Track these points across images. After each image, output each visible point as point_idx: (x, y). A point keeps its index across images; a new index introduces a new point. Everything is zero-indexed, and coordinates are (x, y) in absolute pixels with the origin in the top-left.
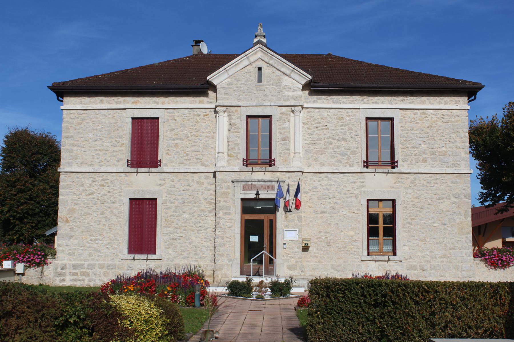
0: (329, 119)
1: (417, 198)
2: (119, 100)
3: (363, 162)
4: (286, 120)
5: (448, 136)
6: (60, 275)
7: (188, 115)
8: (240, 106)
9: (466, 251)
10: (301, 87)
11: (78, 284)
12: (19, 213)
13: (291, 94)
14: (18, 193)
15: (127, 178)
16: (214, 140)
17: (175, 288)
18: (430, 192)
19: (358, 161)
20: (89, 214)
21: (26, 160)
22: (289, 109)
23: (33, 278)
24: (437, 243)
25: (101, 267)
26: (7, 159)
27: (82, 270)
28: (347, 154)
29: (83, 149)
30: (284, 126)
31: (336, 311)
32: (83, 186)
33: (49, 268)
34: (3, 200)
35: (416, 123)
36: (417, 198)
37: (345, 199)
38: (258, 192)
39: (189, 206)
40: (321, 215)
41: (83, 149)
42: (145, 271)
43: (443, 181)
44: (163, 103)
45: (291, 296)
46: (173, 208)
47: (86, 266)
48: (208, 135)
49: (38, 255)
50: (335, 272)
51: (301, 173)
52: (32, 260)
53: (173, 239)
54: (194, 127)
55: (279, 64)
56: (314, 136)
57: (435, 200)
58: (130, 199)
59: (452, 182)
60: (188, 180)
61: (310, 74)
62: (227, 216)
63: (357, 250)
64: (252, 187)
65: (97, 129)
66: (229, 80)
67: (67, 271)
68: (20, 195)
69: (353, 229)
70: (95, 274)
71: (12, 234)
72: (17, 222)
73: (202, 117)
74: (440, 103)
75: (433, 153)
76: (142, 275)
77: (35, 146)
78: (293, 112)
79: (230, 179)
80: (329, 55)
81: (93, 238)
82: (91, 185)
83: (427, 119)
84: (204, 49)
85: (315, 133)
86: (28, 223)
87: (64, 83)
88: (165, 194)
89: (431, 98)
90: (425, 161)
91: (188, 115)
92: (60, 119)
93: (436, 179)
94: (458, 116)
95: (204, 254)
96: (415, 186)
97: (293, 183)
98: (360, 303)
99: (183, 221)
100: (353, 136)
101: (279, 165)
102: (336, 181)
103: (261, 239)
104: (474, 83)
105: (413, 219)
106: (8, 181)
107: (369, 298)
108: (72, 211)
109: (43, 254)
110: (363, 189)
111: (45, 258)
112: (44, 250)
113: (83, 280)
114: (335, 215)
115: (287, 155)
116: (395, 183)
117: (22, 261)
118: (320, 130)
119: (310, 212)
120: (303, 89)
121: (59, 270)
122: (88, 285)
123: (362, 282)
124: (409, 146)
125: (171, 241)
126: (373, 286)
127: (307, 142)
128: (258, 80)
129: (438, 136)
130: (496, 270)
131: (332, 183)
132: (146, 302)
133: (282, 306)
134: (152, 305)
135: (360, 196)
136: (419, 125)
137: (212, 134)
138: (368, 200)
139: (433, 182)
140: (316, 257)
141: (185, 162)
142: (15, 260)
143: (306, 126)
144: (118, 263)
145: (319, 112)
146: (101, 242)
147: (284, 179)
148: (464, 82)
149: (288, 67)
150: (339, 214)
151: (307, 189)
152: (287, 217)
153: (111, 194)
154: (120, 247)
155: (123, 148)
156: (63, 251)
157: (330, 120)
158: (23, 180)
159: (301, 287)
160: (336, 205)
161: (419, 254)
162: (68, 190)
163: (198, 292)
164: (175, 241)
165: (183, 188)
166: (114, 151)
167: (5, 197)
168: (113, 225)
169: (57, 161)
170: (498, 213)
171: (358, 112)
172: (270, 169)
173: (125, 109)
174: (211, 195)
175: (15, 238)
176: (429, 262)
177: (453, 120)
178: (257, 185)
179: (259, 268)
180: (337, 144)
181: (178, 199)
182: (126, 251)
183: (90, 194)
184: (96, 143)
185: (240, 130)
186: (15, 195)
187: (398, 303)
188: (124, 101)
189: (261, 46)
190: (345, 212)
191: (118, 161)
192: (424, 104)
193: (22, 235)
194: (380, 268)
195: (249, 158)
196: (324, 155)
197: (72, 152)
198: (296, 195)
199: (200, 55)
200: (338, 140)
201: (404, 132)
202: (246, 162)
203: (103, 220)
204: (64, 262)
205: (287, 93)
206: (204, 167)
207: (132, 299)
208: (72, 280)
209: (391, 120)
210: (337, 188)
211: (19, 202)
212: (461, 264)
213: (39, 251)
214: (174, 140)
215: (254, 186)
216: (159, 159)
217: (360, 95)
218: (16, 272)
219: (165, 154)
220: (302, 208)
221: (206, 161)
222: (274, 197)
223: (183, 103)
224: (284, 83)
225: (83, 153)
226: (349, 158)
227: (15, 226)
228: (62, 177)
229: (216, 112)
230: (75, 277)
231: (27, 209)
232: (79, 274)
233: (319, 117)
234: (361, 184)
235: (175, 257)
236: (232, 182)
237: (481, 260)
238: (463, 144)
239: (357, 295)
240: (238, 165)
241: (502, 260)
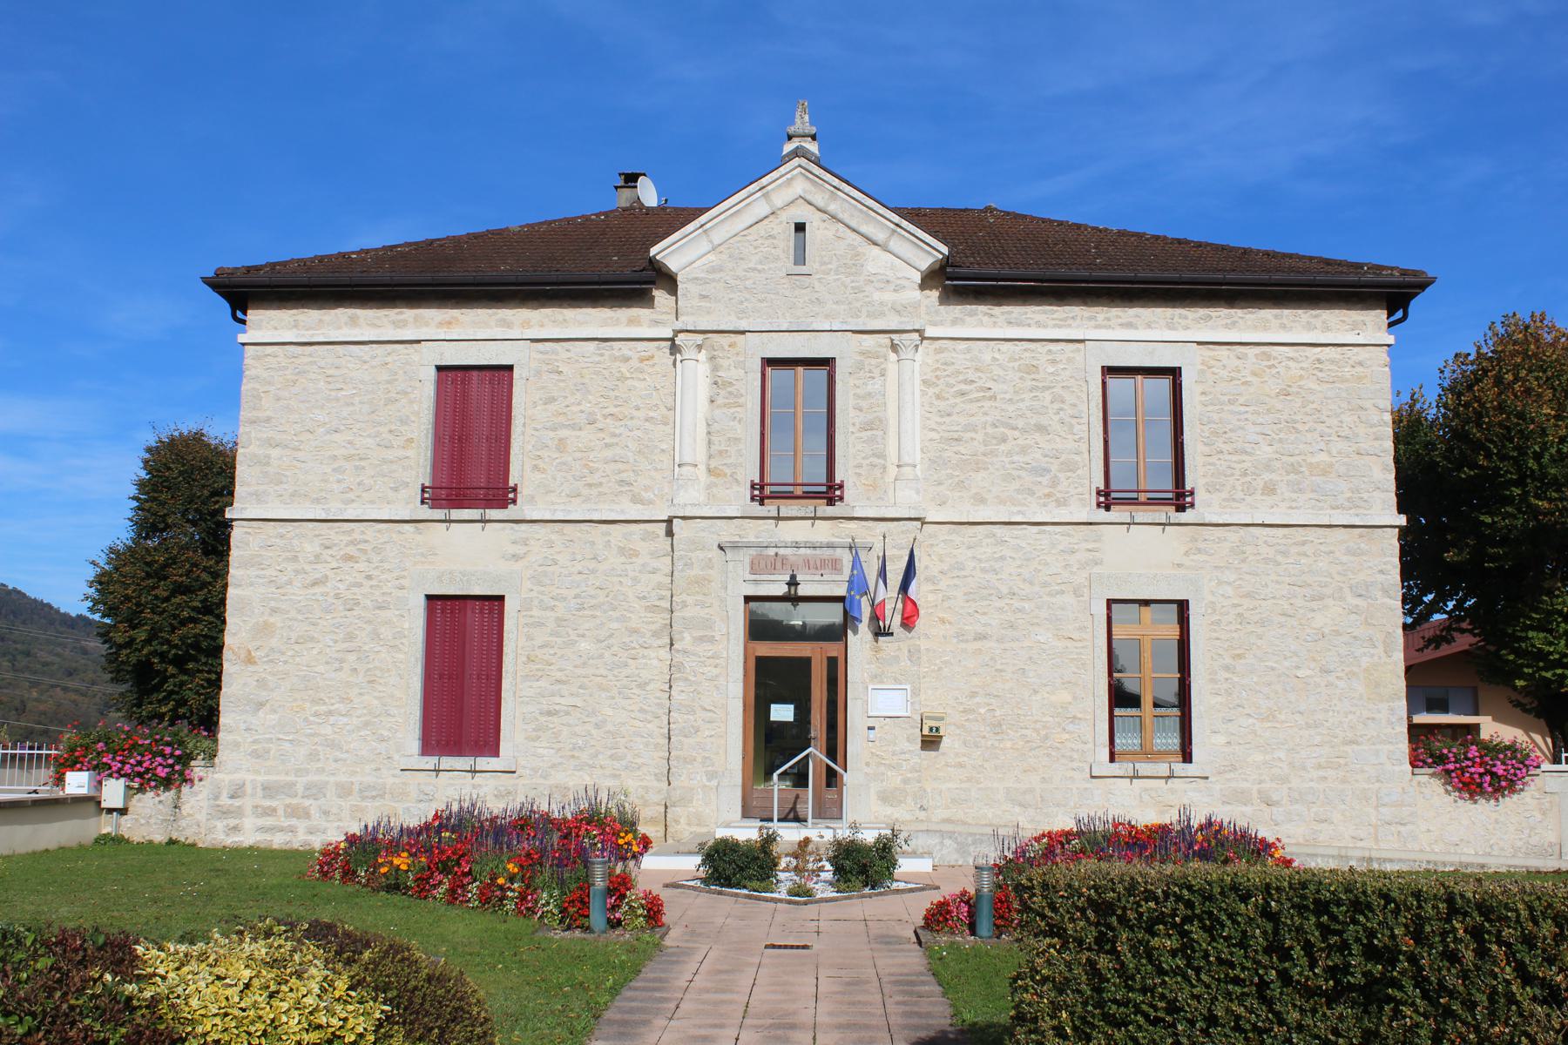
0: (997, 371)
1: (1248, 595)
2: (401, 317)
4: (877, 372)
5: (1335, 422)
6: (225, 813)
7: (598, 359)
8: (743, 332)
9: (1391, 748)
10: (917, 278)
11: (278, 841)
12: (176, 646)
13: (888, 296)
14: (173, 594)
15: (419, 538)
16: (668, 429)
17: (530, 863)
18: (1288, 580)
19: (1080, 490)
20: (312, 639)
21: (196, 510)
22: (884, 339)
23: (152, 821)
24: (1308, 726)
25: (344, 791)
26: (147, 505)
27: (288, 801)
28: (1049, 471)
29: (300, 455)
30: (869, 388)
31: (1146, 1016)
32: (295, 559)
33: (196, 794)
34: (135, 612)
35: (1245, 383)
36: (1248, 595)
37: (1046, 598)
38: (793, 577)
40: (978, 645)
41: (300, 455)
42: (455, 808)
43: (1322, 548)
44: (526, 324)
45: (895, 885)
47: (300, 789)
48: (652, 414)
49: (164, 756)
50: (1017, 809)
51: (918, 524)
52: (148, 770)
53: (549, 713)
54: (612, 394)
55: (856, 213)
56: (955, 417)
57: (1299, 602)
58: (429, 598)
59: (1349, 552)
60: (593, 543)
61: (944, 241)
64: (777, 563)
65: (337, 400)
66: (711, 257)
67: (247, 803)
68: (177, 600)
70: (326, 813)
71: (159, 701)
72: (171, 670)
73: (635, 363)
74: (1309, 327)
75: (1294, 469)
76: (448, 819)
77: (219, 474)
78: (894, 347)
80: (989, 209)
81: (324, 708)
82: (317, 557)
83: (1274, 371)
84: (648, 193)
85: (957, 409)
86: (199, 671)
87: (249, 269)
89: (1286, 312)
90: (1270, 489)
91: (598, 359)
93: (1304, 543)
94: (1360, 364)
95: (638, 755)
96: (1243, 561)
97: (895, 552)
98: (1263, 985)
100: (1067, 419)
101: (855, 499)
103: (803, 713)
104: (1404, 273)
105: (1239, 656)
106: (147, 564)
107: (1304, 961)
108: (264, 629)
109: (178, 753)
111: (186, 765)
112: (181, 743)
113: (292, 830)
115: (877, 472)
116: (1186, 553)
117: (120, 774)
118: (971, 401)
120: (924, 285)
121: (225, 801)
122: (306, 843)
123: (1268, 886)
124: (1225, 447)
126: (1321, 907)
127: (933, 435)
128: (797, 256)
129: (1306, 419)
130: (1476, 802)
132: (317, 972)
133: (875, 929)
134: (341, 985)
136: (1252, 390)
137: (664, 411)
138: (1110, 603)
139: (1294, 550)
140: (961, 765)
141: (585, 491)
142: (101, 770)
143: (931, 391)
144: (391, 780)
145: (969, 350)
146: (345, 720)
147: (869, 539)
148: (1379, 268)
149: (880, 224)
152: (877, 650)
153: (374, 583)
154: (399, 735)
155: (411, 453)
156: (237, 745)
157: (1002, 373)
158: (187, 560)
159: (921, 856)
160: (1019, 615)
161: (1259, 757)
162: (253, 572)
163: (599, 883)
164: (555, 719)
165: (579, 567)
166: (384, 461)
167: (138, 604)
168: (378, 673)
169: (226, 492)
170: (1426, 647)
171: (1079, 350)
173: (418, 342)
174: (659, 586)
175: (164, 709)
176: (1284, 780)
177: (1348, 375)
178: (792, 559)
179: (797, 797)
180: (1019, 442)
181: (565, 599)
182: (415, 745)
183: (314, 584)
184: (336, 437)
185: (741, 400)
186: (167, 599)
187: (1452, 994)
188: (416, 319)
189: (803, 161)
191: (396, 490)
192: (1266, 329)
193: (183, 702)
194: (1146, 797)
195: (768, 480)
196: (982, 474)
197: (268, 464)
199: (636, 211)
200: (1024, 431)
201: (1210, 408)
202: (761, 492)
203: (352, 657)
204: (238, 777)
205: (877, 296)
207: (243, 959)
208: (261, 829)
209: (1174, 373)
211: (175, 617)
212: (1377, 785)
213: (168, 744)
214: (554, 429)
215: (784, 560)
216: (511, 484)
217: (1085, 304)
218: (104, 805)
219: (527, 468)
220: (921, 623)
221: (647, 488)
222: (841, 591)
223: (581, 324)
224: (870, 268)
225: (299, 465)
226: (1054, 483)
227: (165, 680)
228: (237, 534)
229: (674, 349)
230: (269, 821)
231: (195, 636)
232: (281, 812)
233: (969, 364)
234: (1089, 555)
235: (553, 766)
236: (721, 548)
237: (1432, 775)
238: (1377, 444)
239: (1242, 944)
240: (738, 499)
241: (1493, 775)
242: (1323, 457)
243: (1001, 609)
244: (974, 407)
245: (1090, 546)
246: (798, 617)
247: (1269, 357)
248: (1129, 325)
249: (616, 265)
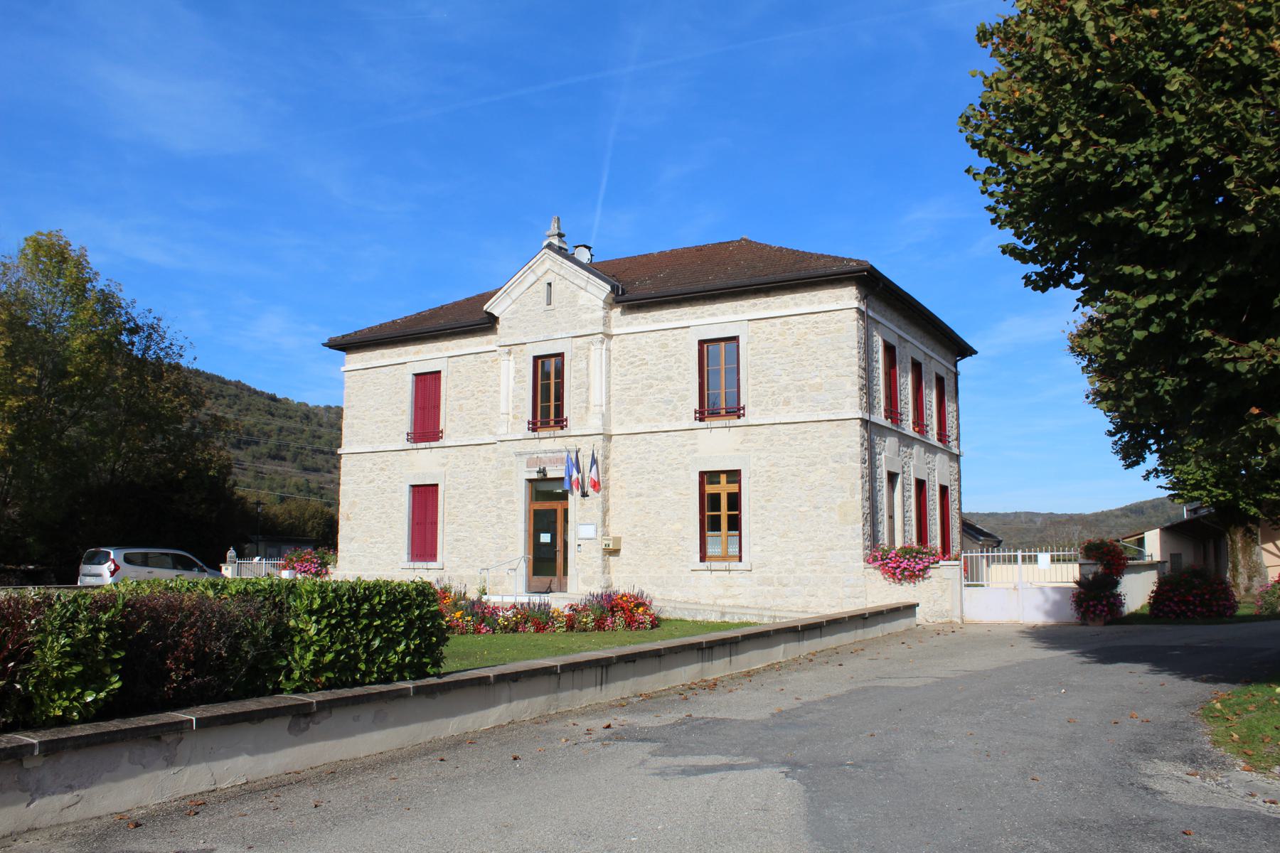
10: (601, 304)
13: (588, 316)
24: (806, 540)
44: (447, 349)
53: (457, 540)
59: (831, 436)
73: (490, 364)
90: (787, 402)
92: (341, 384)
101: (573, 426)
103: (554, 538)
108: (353, 504)
124: (764, 380)
139: (800, 437)
161: (778, 558)
222: (562, 475)
226: (675, 408)
240: (523, 430)
242: (818, 380)
244: (636, 370)
247: (787, 323)
248: (713, 315)
249: (477, 318)
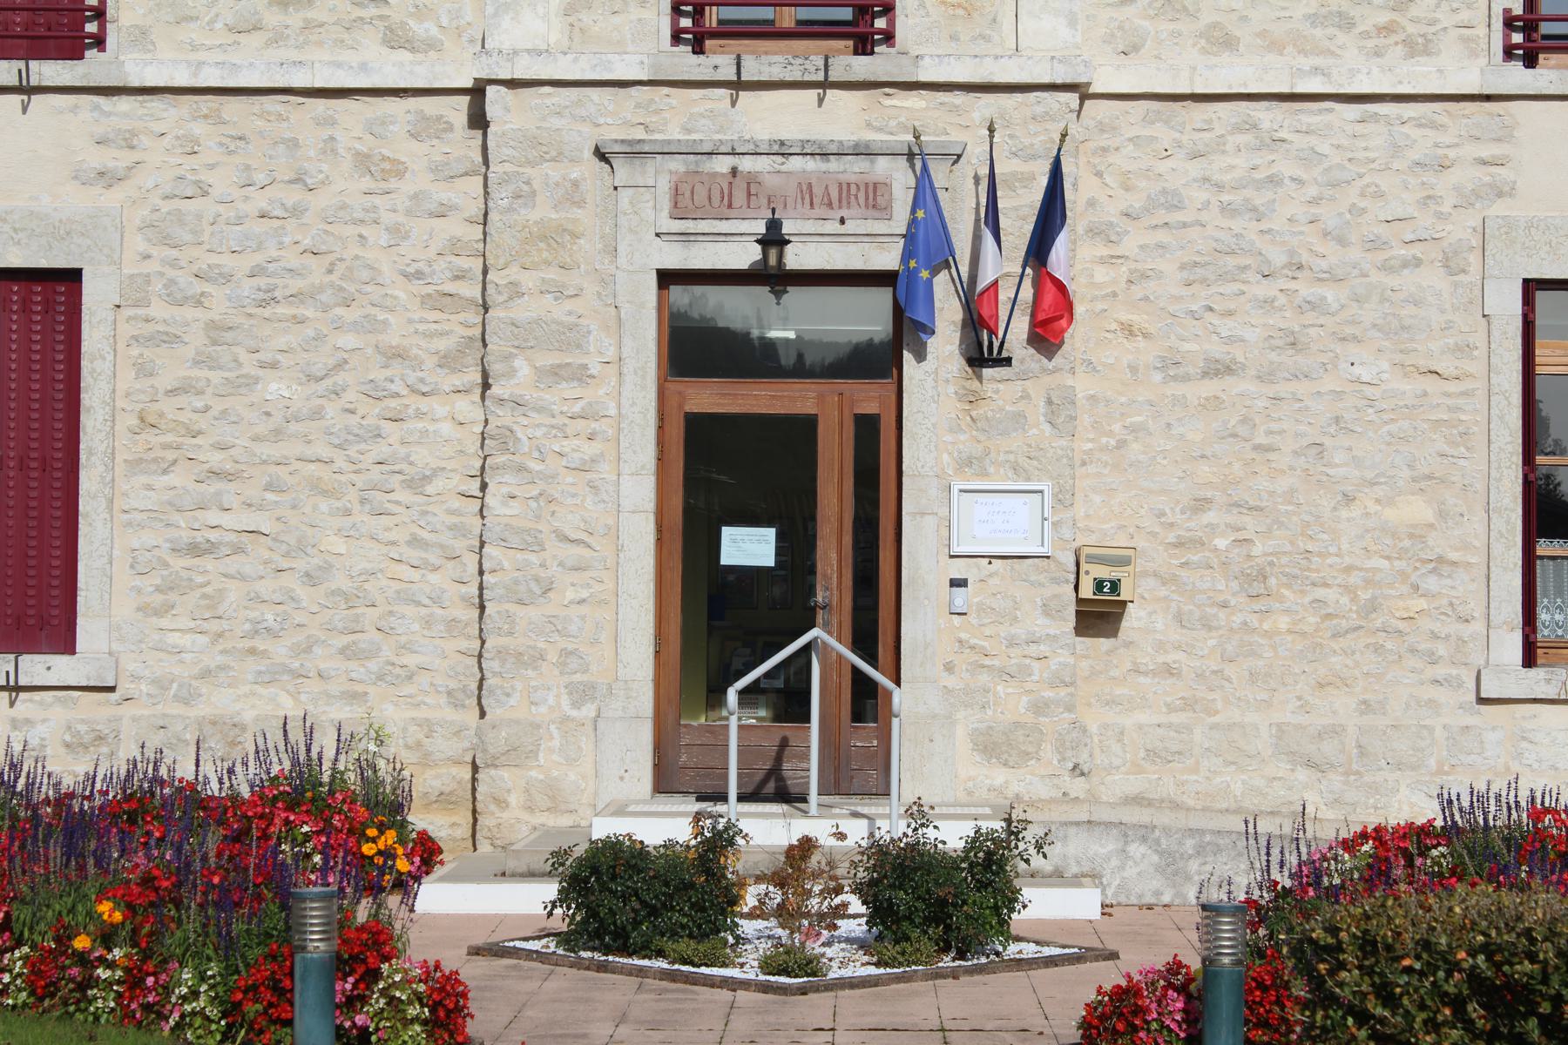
3: (1498, 24)
17: (151, 901)
19: (1464, 16)
37: (1375, 277)
38: (774, 225)
39: (301, 321)
40: (1210, 387)
45: (1013, 950)
46: (196, 340)
50: (1302, 775)
51: (1072, 99)
53: (195, 550)
60: (293, 144)
62: (569, 389)
63: (1453, 628)
64: (736, 191)
69: (1425, 482)
79: (583, 139)
88: (138, 243)
99: (261, 429)
102: (1311, 157)
110: (1499, 209)
114: (1302, 388)
119: (1133, 369)
125: (178, 563)
131: (1286, 168)
135: (1474, 259)
138: (1531, 287)
140: (1169, 671)
147: (956, 136)
150: (1329, 384)
151: (1110, 211)
152: (973, 399)
159: (1076, 881)
160: (1310, 318)
163: (317, 943)
164: (208, 563)
165: (260, 201)
172: (861, 67)
174: (455, 247)
178: (771, 182)
179: (784, 744)
181: (228, 278)
190: (1370, 366)
198: (1039, 249)
206: (404, 56)
210: (1314, 201)
215: (752, 181)
220: (1077, 336)
222: (887, 258)
234: (1484, 175)
235: (206, 674)
236: (601, 155)
243: (1268, 302)
245: (1486, 152)
246: (784, 322)
